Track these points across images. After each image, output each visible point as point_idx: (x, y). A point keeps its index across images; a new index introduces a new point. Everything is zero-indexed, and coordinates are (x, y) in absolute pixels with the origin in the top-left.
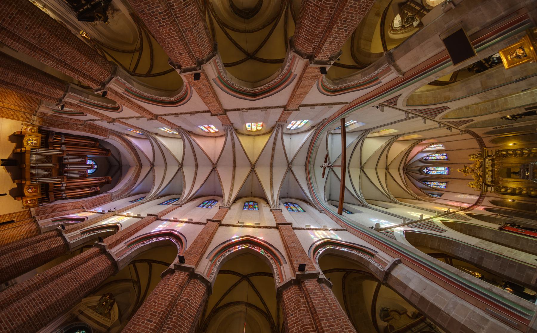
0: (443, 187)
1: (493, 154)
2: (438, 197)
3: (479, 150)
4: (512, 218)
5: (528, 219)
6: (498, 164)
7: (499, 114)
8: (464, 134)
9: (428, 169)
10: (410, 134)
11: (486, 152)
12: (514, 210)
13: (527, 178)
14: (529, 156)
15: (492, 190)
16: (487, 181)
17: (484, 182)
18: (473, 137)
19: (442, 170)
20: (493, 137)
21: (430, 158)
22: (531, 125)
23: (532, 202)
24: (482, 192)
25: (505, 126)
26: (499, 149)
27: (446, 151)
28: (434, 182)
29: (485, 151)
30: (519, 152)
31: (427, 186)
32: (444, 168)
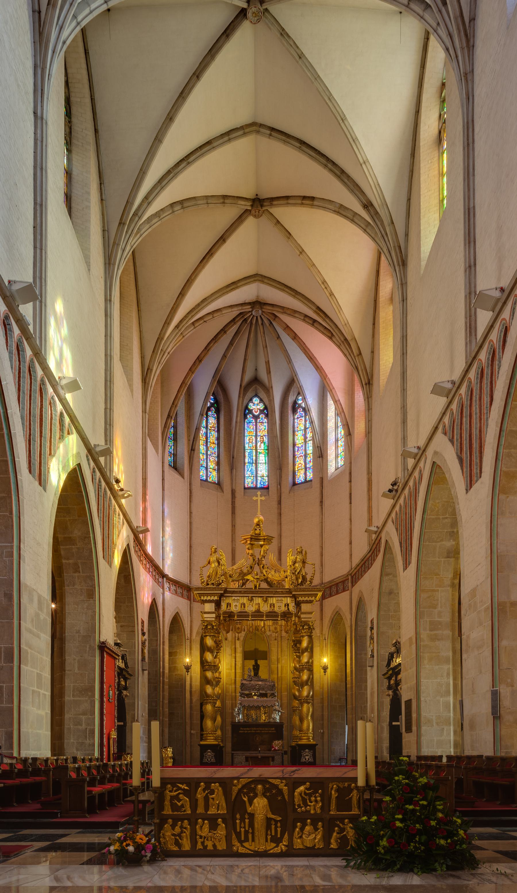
0: (202, 473)
1: (302, 616)
2: (169, 459)
3: (316, 581)
4: (143, 670)
5: (147, 705)
6: (276, 628)
7: (410, 639)
8: (370, 536)
9: (262, 416)
10: (399, 329)
11: (310, 598)
12: (163, 672)
13: (242, 695)
14: (295, 697)
15: (206, 615)
16: (230, 600)
17: (226, 593)
18: (354, 565)
19: (259, 469)
20: (348, 616)
21: (300, 424)
22: (366, 707)
23: (191, 708)
24: (197, 589)
25: (372, 651)
26: (316, 633)
27: (322, 479)
28: (218, 439)
29: (311, 595)
30: (305, 677)
31: (201, 415)
32: (265, 473)
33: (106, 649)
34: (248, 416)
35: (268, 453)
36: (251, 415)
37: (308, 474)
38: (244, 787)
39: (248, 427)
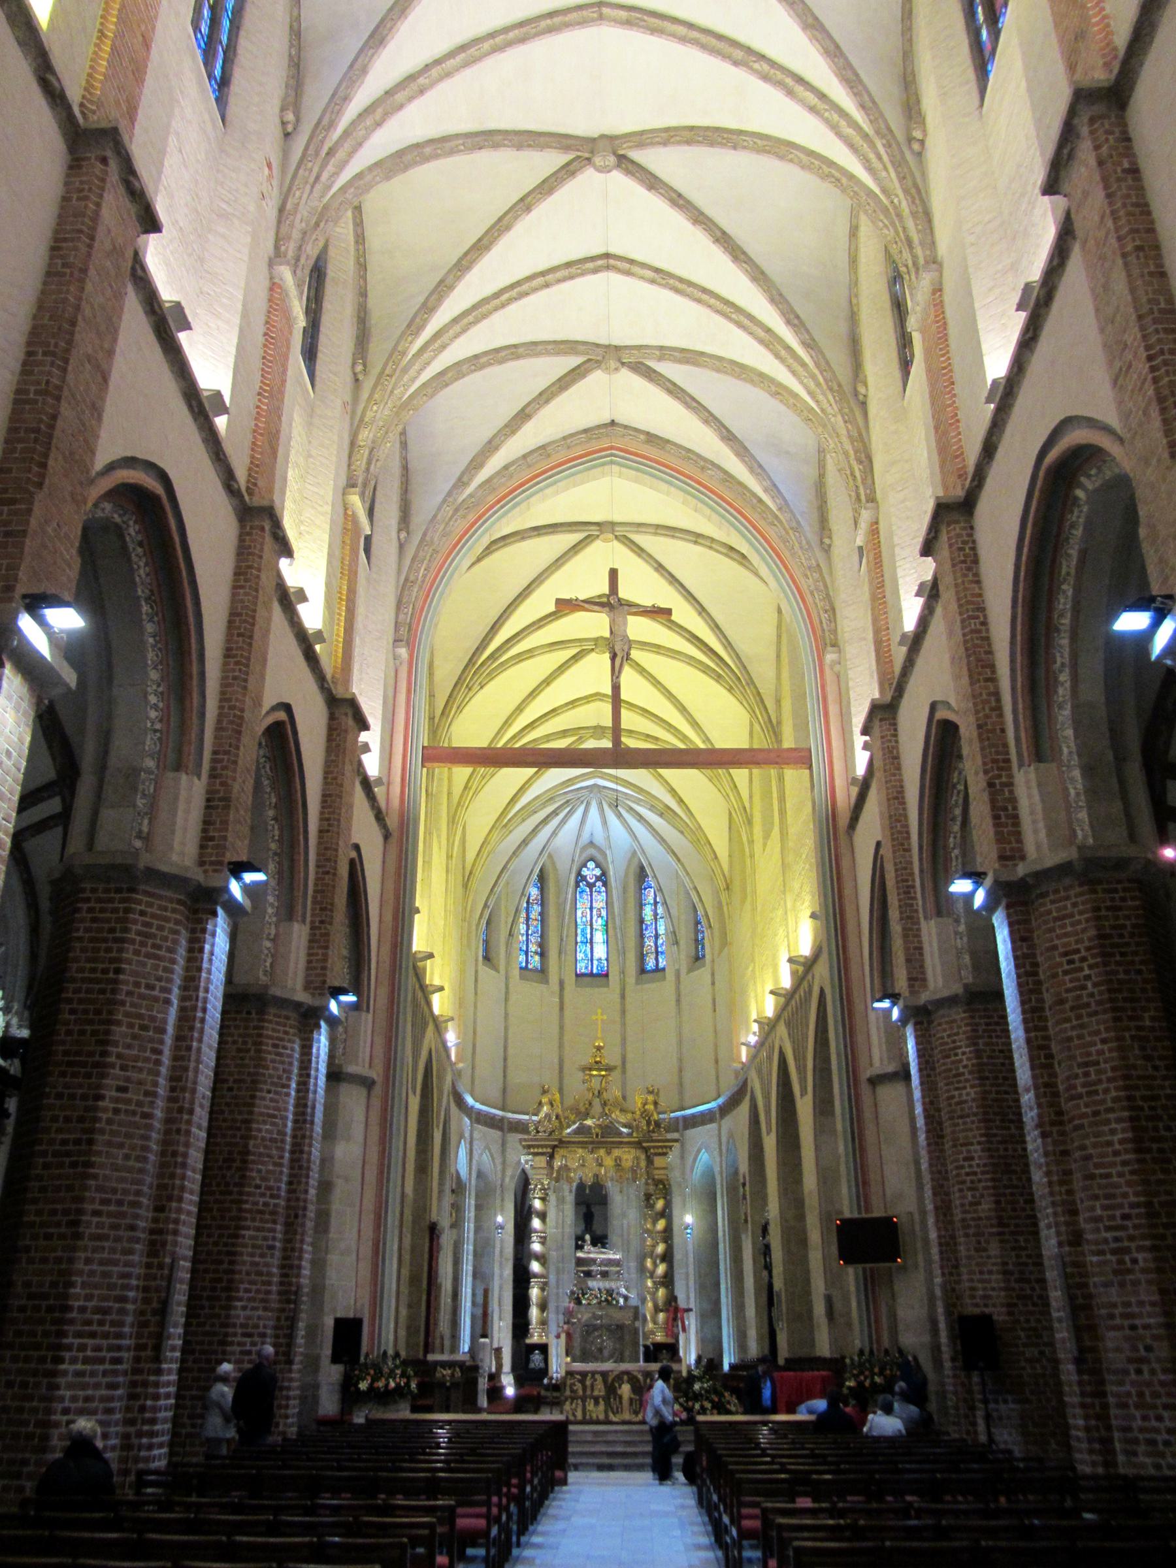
9: (599, 884)
32: (604, 956)
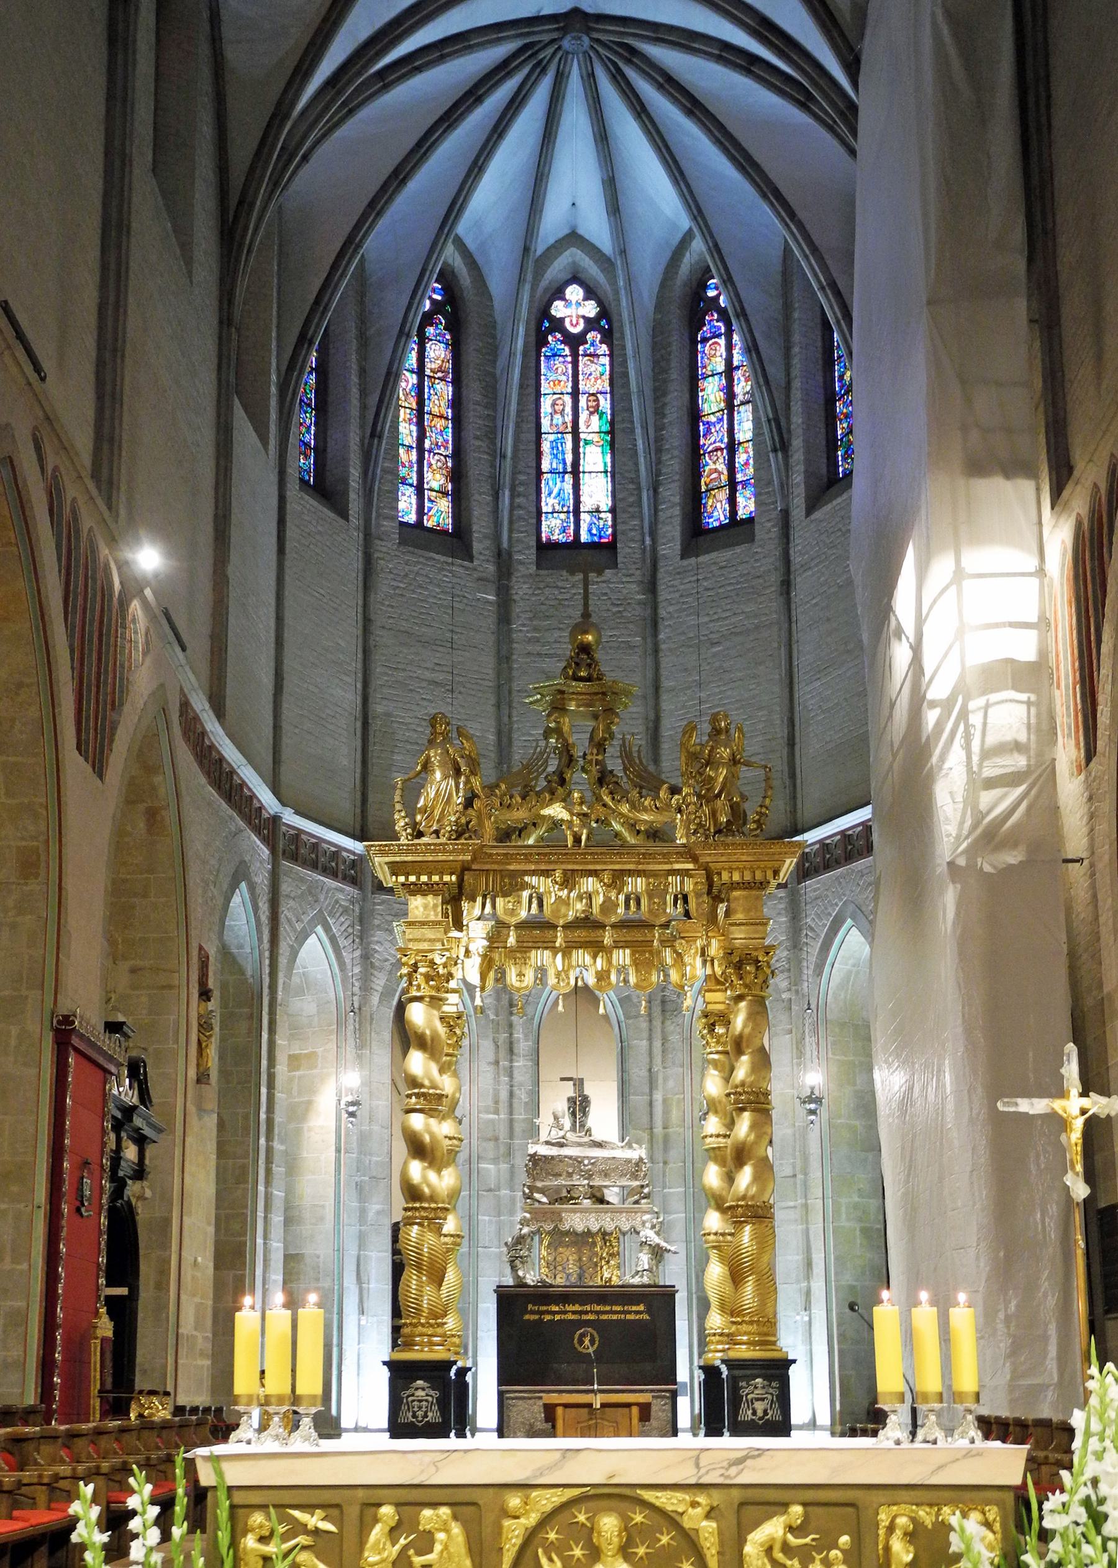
19: (584, 489)
28: (456, 403)
32: (605, 503)
33: (75, 1041)
34: (550, 338)
35: (612, 444)
36: (559, 336)
37: (740, 499)
38: (545, 1521)
39: (549, 368)
